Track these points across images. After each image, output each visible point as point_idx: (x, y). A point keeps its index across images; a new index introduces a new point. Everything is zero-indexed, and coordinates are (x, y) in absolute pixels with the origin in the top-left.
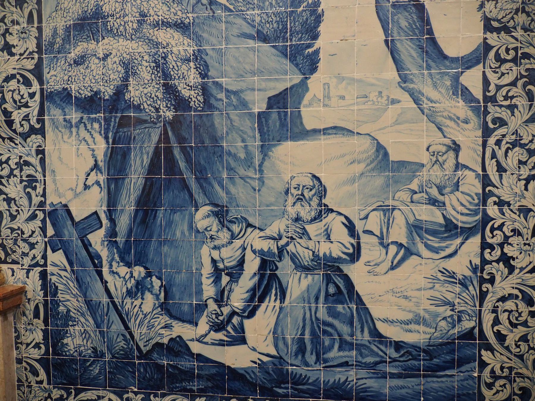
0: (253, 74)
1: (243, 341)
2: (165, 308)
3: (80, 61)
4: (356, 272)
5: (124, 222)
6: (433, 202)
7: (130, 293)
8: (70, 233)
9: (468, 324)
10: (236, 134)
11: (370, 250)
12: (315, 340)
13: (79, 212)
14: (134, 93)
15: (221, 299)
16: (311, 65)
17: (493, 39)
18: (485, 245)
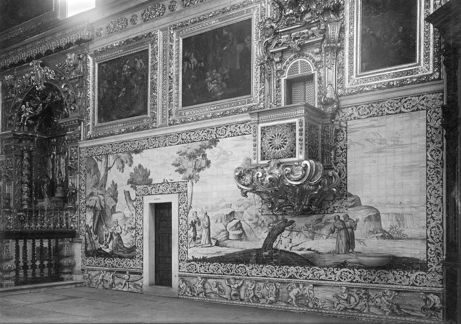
0: (110, 202)
1: (108, 247)
2: (99, 242)
3: (90, 200)
4: (121, 235)
5: (95, 227)
6: (130, 224)
7: (95, 240)
8: (89, 229)
9: (134, 244)
10: (108, 212)
11: (123, 232)
12: (116, 247)
13: (90, 226)
14: (97, 206)
15: (106, 241)
16: (116, 201)
17: (137, 197)
18: (136, 231)
